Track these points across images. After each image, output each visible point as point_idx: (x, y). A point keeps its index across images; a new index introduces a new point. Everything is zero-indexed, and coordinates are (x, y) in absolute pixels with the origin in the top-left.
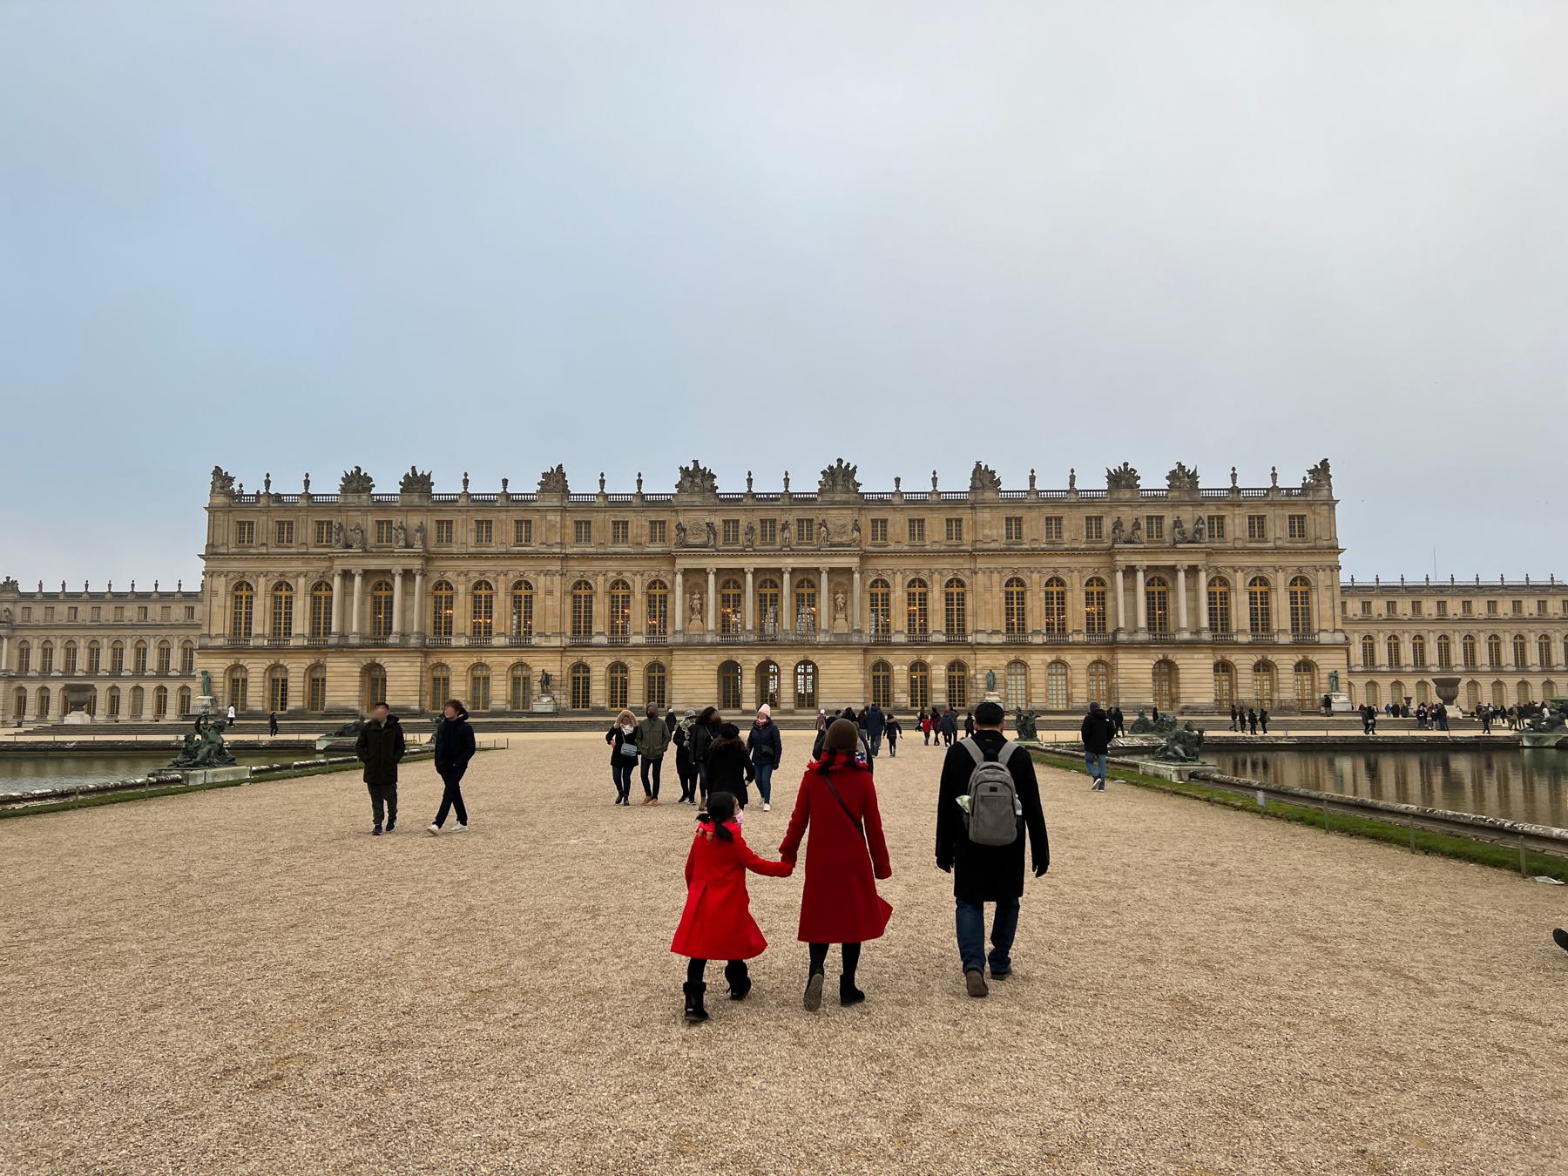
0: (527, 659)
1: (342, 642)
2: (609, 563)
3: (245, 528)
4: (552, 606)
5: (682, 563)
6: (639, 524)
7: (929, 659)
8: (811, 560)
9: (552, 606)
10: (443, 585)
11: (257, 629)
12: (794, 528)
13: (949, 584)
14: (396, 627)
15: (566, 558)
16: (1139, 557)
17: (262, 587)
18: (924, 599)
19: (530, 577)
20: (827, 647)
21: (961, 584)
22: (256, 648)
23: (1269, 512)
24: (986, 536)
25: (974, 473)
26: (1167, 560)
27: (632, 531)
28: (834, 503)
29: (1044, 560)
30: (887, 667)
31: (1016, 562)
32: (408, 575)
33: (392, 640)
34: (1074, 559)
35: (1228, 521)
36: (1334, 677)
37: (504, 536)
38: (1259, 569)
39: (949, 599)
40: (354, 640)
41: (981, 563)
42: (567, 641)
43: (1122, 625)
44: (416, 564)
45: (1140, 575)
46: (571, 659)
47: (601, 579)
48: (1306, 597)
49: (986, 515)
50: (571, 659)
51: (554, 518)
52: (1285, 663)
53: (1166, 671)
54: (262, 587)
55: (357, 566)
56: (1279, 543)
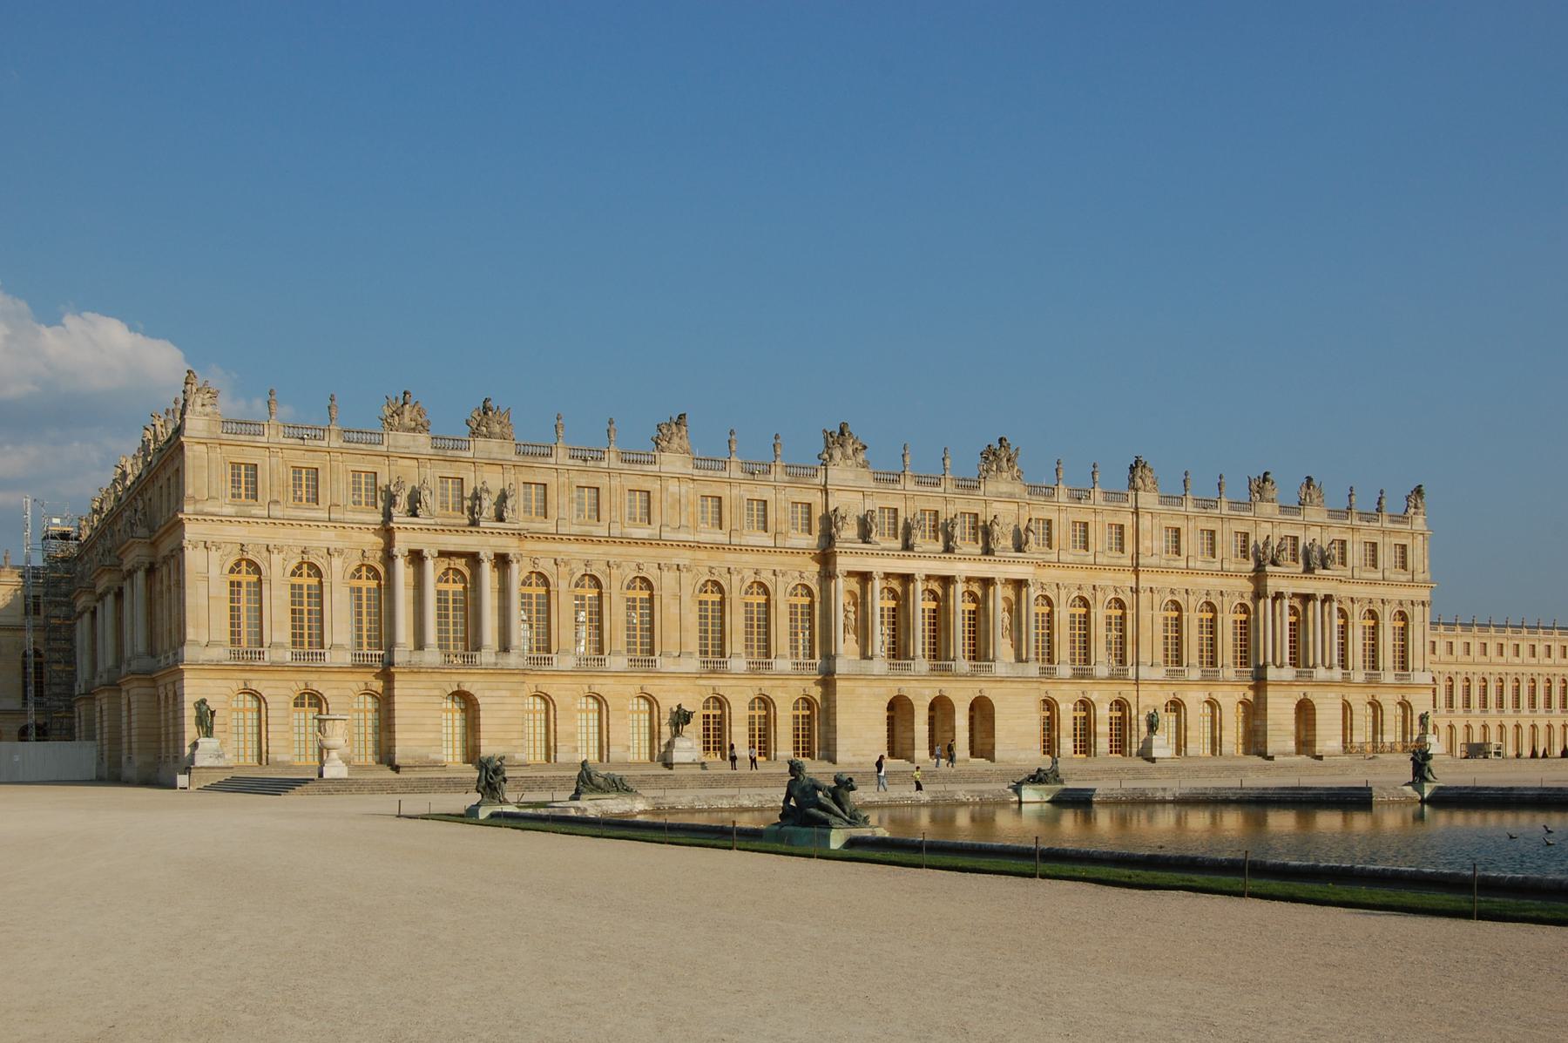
0: (653, 687)
2: (746, 557)
15: (698, 546)
19: (651, 573)
20: (1002, 680)
21: (1121, 604)
22: (273, 664)
25: (1132, 469)
26: (1307, 586)
28: (999, 495)
29: (1201, 580)
30: (1049, 705)
31: (1174, 581)
32: (502, 561)
33: (488, 656)
34: (1225, 581)
35: (1349, 546)
36: (1423, 718)
38: (1370, 602)
41: (1145, 581)
43: (1270, 659)
47: (736, 578)
52: (1389, 701)
53: (1305, 711)
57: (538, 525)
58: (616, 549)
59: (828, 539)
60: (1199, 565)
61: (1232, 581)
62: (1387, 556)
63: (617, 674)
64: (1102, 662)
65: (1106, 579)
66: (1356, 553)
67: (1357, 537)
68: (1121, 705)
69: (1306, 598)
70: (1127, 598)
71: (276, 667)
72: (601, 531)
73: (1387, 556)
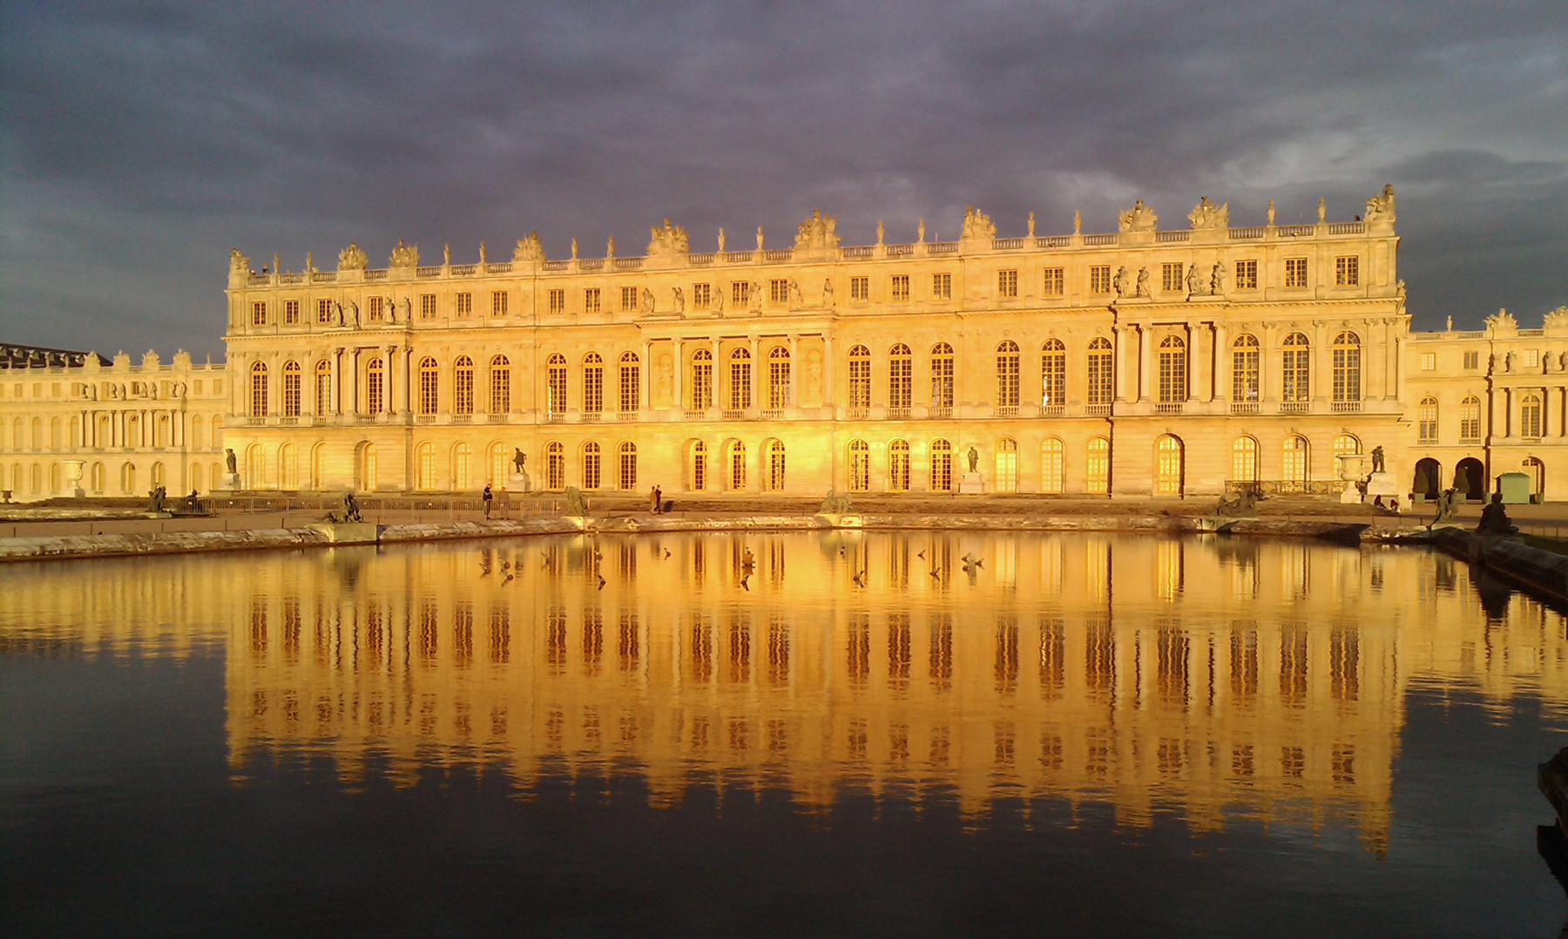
1: (339, 420)
2: (581, 334)
4: (528, 380)
5: (649, 332)
8: (778, 326)
9: (528, 380)
11: (271, 409)
12: (765, 293)
14: (386, 405)
16: (1143, 313)
18: (907, 366)
24: (975, 294)
27: (603, 298)
29: (1041, 318)
33: (381, 417)
36: (1378, 455)
42: (540, 419)
44: (400, 341)
45: (1146, 335)
48: (1355, 356)
49: (974, 267)
51: (527, 286)
55: (351, 342)
56: (1321, 292)
57: (429, 324)
58: (480, 336)
60: (1038, 304)
61: (1083, 317)
62: (1322, 273)
66: (1272, 272)
67: (1275, 254)
73: (1322, 273)
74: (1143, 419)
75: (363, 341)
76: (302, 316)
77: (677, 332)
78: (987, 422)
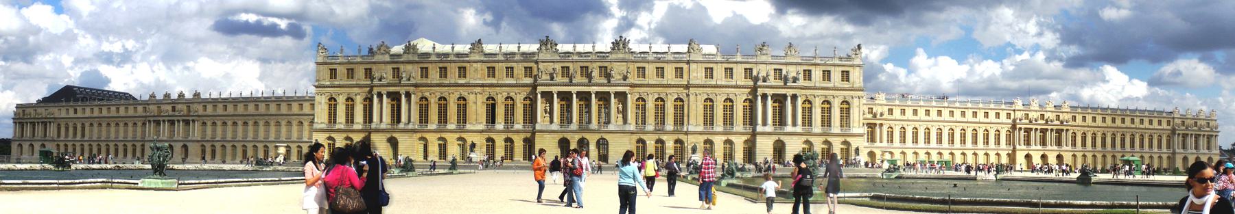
3: (333, 74)
4: (477, 109)
6: (519, 69)
7: (664, 138)
9: (477, 109)
10: (424, 98)
13: (676, 100)
15: (482, 85)
17: (341, 100)
18: (663, 107)
19: (465, 94)
21: (682, 100)
23: (831, 69)
32: (408, 95)
33: (401, 126)
36: (857, 150)
37: (453, 77)
39: (676, 107)
40: (383, 126)
44: (411, 89)
46: (486, 135)
49: (693, 66)
50: (486, 135)
54: (341, 100)
55: (384, 91)
57: (424, 81)
59: (535, 80)
63: (451, 131)
64: (669, 126)
65: (674, 90)
68: (678, 141)
69: (785, 96)
70: (685, 99)
71: (339, 131)
72: (447, 82)
74: (769, 134)
75: (392, 89)
76: (356, 76)
77: (555, 89)
78: (701, 133)
